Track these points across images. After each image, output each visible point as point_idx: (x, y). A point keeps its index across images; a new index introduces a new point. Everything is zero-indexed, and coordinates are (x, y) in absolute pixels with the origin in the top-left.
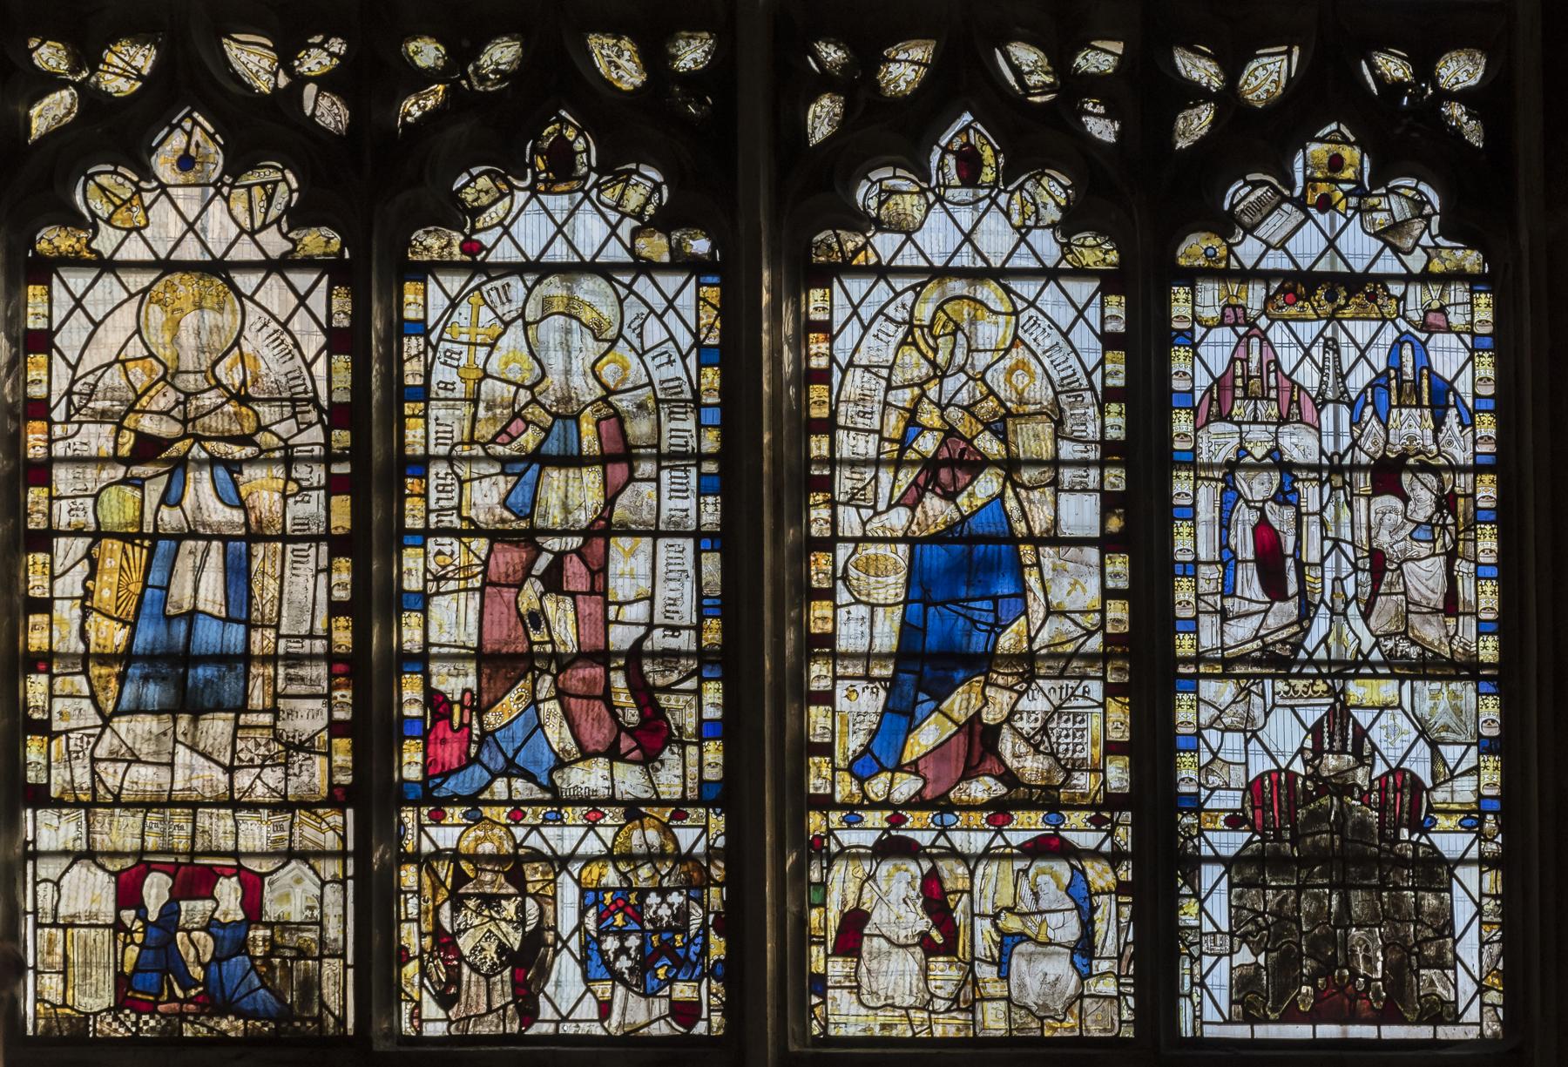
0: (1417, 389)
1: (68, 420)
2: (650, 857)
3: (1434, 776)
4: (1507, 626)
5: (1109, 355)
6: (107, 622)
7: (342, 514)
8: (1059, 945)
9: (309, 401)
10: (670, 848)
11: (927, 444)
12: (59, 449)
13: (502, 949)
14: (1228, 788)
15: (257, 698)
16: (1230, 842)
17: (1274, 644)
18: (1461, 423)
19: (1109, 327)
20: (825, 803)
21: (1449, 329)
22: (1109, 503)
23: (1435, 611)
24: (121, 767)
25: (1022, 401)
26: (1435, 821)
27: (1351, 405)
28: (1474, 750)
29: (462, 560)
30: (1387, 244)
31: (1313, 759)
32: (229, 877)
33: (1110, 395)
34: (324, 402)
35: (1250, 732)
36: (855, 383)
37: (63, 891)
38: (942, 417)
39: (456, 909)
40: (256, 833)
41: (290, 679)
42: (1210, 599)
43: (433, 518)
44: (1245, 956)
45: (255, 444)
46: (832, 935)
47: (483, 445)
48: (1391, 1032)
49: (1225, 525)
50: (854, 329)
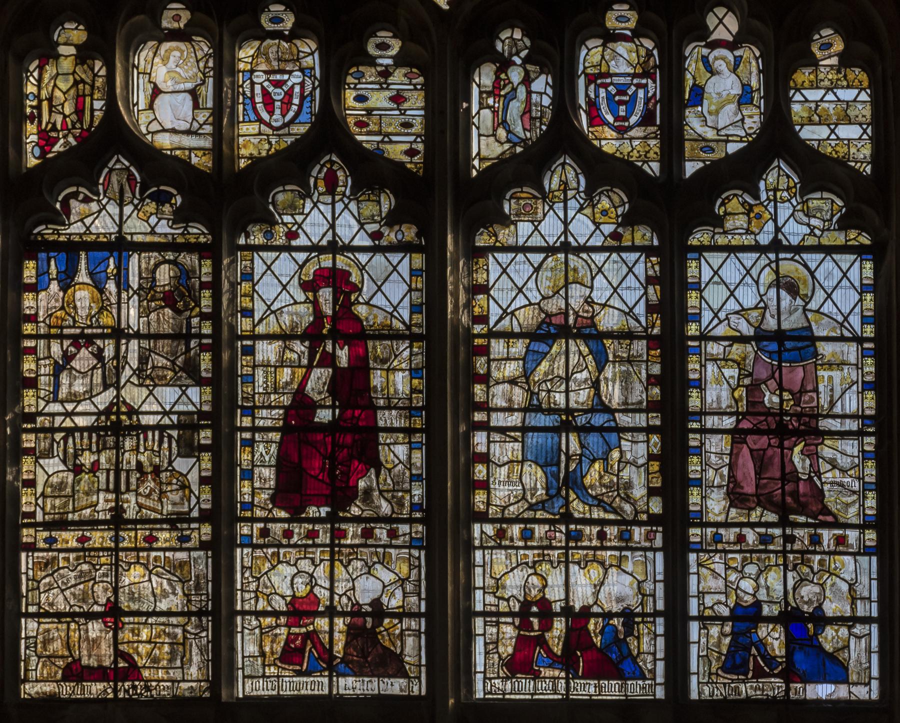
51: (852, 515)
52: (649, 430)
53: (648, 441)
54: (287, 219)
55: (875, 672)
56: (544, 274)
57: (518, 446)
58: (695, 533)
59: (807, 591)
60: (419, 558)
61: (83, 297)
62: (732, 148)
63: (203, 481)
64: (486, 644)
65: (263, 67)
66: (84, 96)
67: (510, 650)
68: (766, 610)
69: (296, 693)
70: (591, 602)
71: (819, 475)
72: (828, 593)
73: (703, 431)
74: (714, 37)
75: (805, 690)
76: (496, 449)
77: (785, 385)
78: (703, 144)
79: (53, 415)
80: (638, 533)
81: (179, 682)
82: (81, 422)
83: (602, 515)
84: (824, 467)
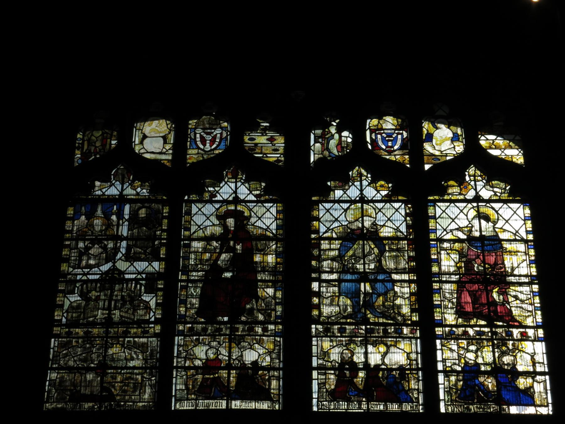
51: (529, 322)
52: (410, 282)
53: (410, 287)
54: (211, 189)
55: (550, 401)
56: (350, 212)
57: (336, 289)
58: (439, 331)
59: (507, 359)
60: (280, 341)
61: (98, 223)
62: (448, 158)
63: (157, 304)
64: (318, 384)
65: (201, 127)
66: (107, 139)
67: (333, 387)
68: (483, 368)
69: (206, 408)
70: (380, 362)
71: (509, 303)
72: (518, 360)
73: (441, 282)
74: (437, 114)
75: (509, 409)
76: (323, 289)
77: (487, 261)
78: (434, 157)
79: (77, 275)
80: (406, 330)
81: (137, 402)
82: (91, 277)
83: (384, 321)
84: (511, 299)
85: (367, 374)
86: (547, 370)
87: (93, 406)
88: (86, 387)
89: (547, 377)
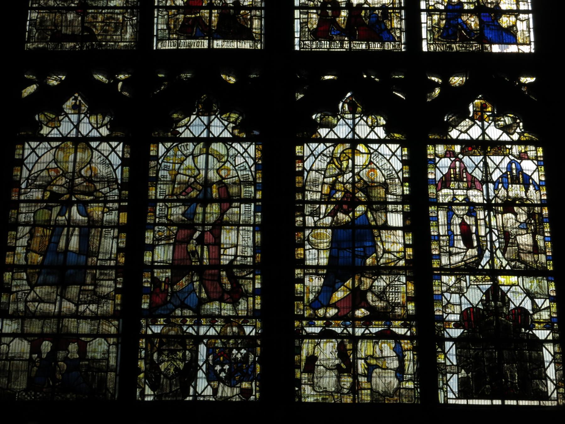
0: (518, 178)
1: (26, 188)
2: (235, 336)
3: (533, 309)
4: (554, 258)
5: (404, 167)
6: (34, 254)
7: (124, 218)
8: (391, 369)
9: (113, 182)
10: (242, 334)
11: (339, 195)
12: (22, 197)
13: (176, 369)
14: (454, 313)
15: (89, 280)
16: (456, 333)
17: (470, 263)
18: (535, 189)
19: (404, 158)
20: (301, 318)
21: (528, 159)
22: (406, 216)
23: (529, 252)
24: (36, 304)
25: (373, 182)
26: (534, 326)
27: (494, 183)
28: (548, 301)
29: (166, 233)
30: (504, 132)
31: (486, 303)
32: (74, 343)
33: (405, 180)
34: (119, 182)
35: (461, 292)
36: (313, 174)
37: (11, 348)
38: (344, 187)
39: (159, 355)
40: (85, 327)
41: (101, 274)
42: (445, 248)
43: (157, 220)
44: (463, 373)
45: (93, 195)
46: (303, 364)
47: (176, 196)
48: (522, 403)
49: (449, 224)
50: (312, 159)
55: (532, 39)
64: (301, 23)
67: (315, 26)
68: (466, 7)
69: (188, 48)
75: (491, 48)
81: (119, 42)
85: (349, 14)
86: (530, 8)
87: (75, 46)
88: (67, 26)
89: (531, 15)
